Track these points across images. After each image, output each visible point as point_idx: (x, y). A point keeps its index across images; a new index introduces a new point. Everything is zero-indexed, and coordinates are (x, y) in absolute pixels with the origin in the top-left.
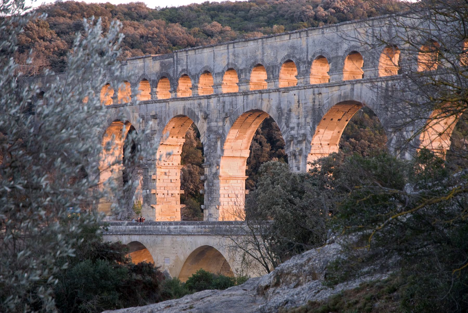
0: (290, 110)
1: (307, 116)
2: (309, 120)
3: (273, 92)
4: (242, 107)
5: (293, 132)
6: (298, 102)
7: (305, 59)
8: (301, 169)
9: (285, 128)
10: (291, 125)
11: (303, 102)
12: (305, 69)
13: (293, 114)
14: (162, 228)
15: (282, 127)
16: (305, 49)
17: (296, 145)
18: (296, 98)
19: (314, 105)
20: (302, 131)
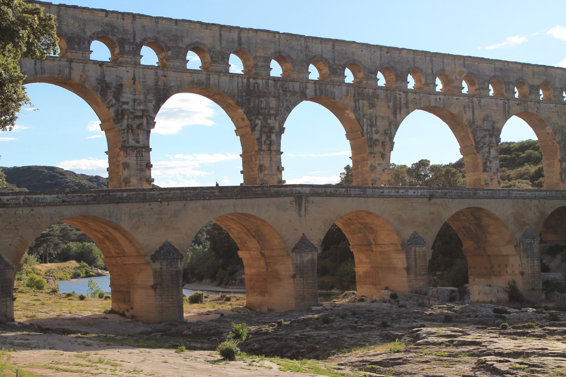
0: (121, 85)
1: (148, 94)
4: (33, 70)
5: (125, 107)
6: (134, 79)
7: (132, 41)
8: (141, 143)
9: (114, 101)
10: (123, 100)
11: (141, 80)
12: (131, 49)
15: (108, 100)
17: (134, 119)
18: (130, 75)
19: (156, 85)
20: (142, 107)
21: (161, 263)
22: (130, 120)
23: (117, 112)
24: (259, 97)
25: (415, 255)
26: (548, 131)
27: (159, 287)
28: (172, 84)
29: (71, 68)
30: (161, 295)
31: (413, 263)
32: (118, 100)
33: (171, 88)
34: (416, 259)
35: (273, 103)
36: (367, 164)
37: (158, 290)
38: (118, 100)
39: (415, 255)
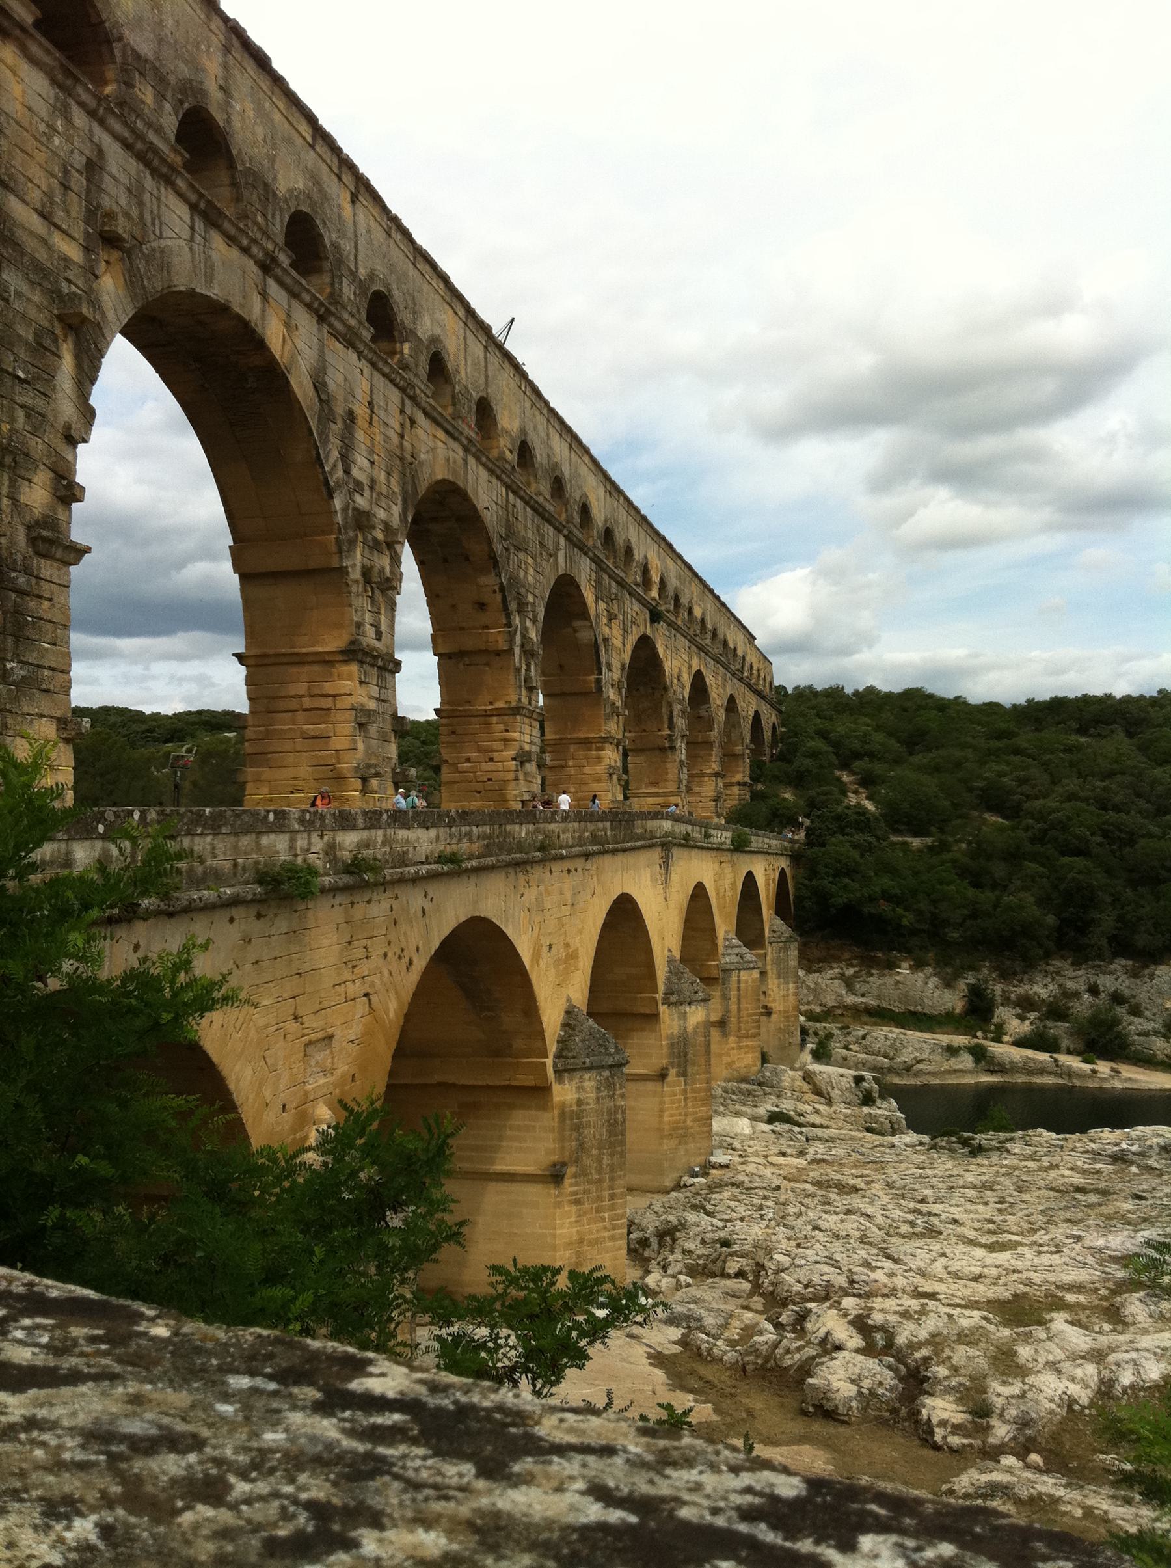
0: (351, 416)
2: (396, 488)
3: (308, 306)
9: (340, 473)
13: (360, 435)
14: (292, 848)
15: (332, 461)
16: (350, 234)
21: (582, 1080)
22: (367, 554)
23: (345, 509)
24: (518, 549)
25: (739, 989)
26: (703, 713)
27: (571, 1170)
28: (423, 457)
29: (264, 295)
30: (577, 1202)
31: (734, 1008)
32: (347, 471)
33: (421, 463)
34: (739, 996)
35: (531, 571)
36: (599, 759)
37: (567, 1181)
38: (347, 471)
39: (739, 989)
